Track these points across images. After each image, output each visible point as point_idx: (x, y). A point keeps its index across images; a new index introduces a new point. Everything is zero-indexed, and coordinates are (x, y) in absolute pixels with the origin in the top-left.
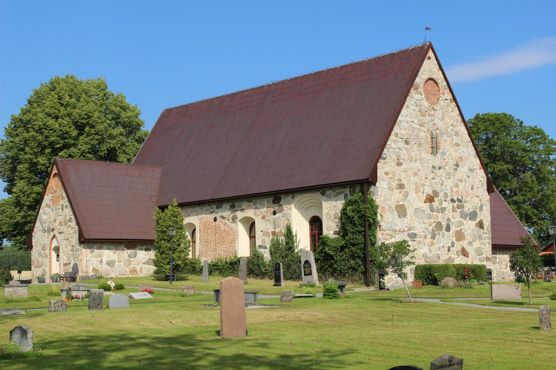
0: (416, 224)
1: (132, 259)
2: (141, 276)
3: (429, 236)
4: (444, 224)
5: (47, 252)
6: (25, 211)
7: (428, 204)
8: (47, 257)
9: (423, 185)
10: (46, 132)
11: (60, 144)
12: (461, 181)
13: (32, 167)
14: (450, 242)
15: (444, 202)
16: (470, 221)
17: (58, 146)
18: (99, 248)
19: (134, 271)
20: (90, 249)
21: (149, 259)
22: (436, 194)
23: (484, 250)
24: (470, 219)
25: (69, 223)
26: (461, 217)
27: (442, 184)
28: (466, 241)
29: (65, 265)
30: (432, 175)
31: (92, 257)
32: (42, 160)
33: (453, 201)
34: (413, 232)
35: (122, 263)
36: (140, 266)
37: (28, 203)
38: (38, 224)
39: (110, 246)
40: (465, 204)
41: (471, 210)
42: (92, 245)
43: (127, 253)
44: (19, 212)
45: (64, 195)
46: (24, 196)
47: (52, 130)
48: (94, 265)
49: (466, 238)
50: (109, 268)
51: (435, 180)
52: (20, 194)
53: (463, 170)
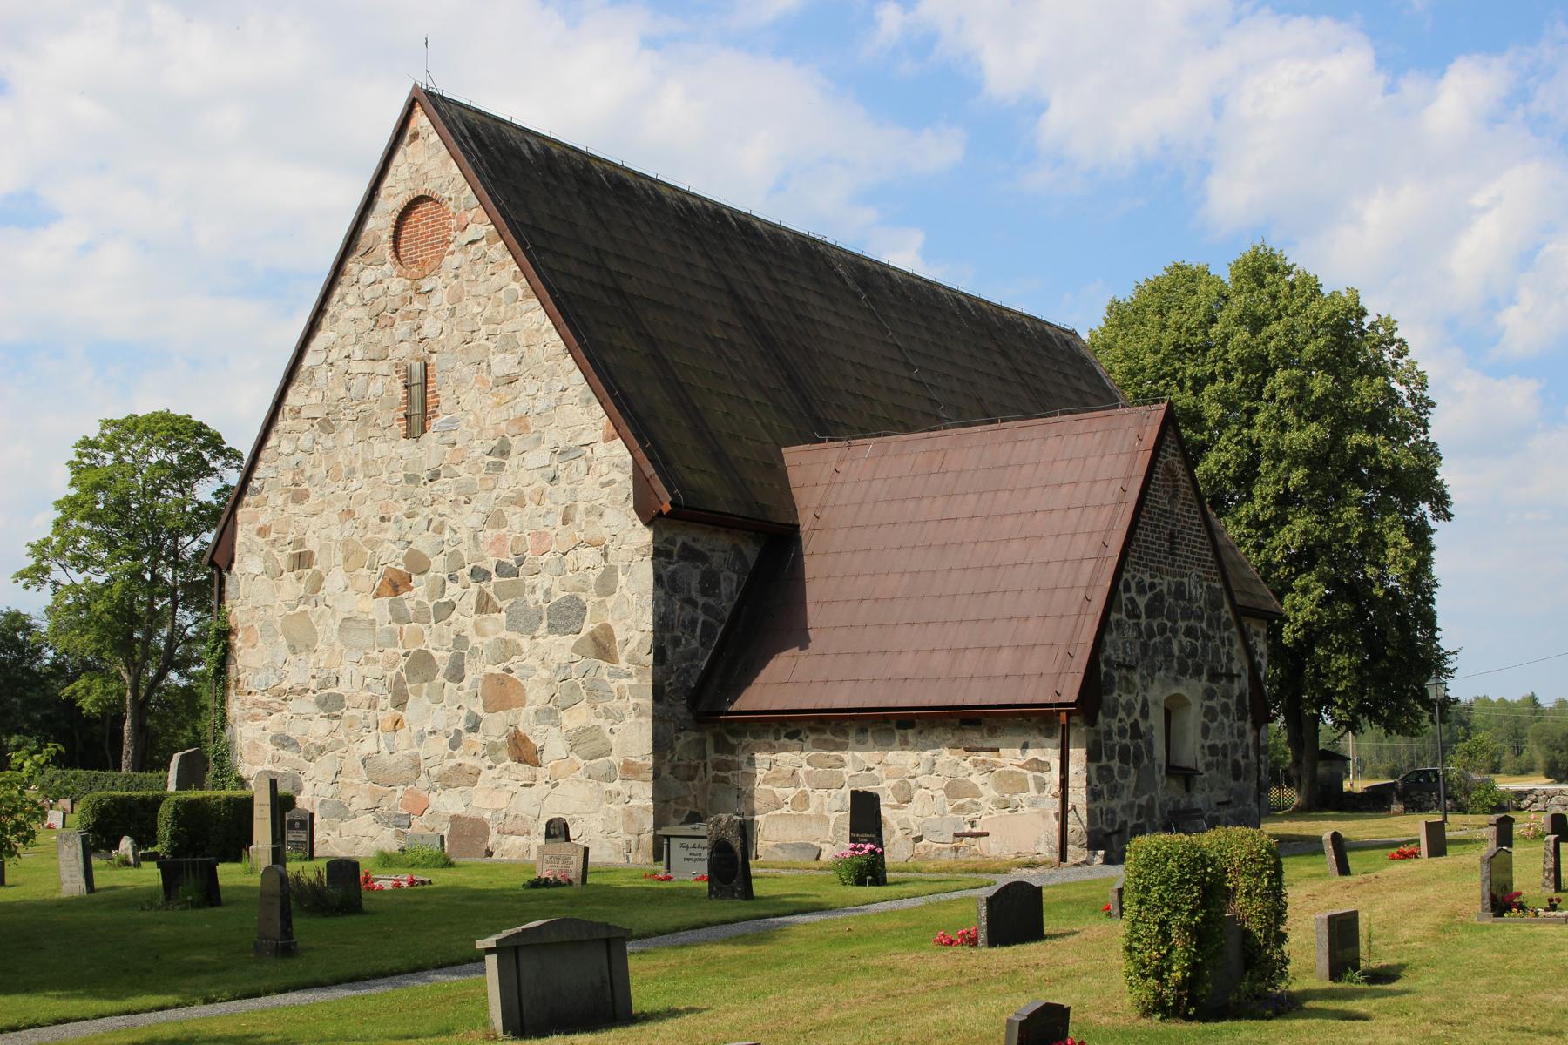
0: (346, 669)
3: (385, 702)
4: (442, 657)
7: (386, 600)
9: (373, 544)
12: (518, 501)
14: (463, 713)
15: (449, 584)
16: (551, 637)
22: (418, 563)
23: (613, 740)
24: (552, 628)
26: (511, 627)
27: (440, 530)
28: (529, 710)
30: (405, 505)
33: (479, 574)
34: (334, 690)
40: (528, 580)
41: (558, 595)
49: (531, 697)
51: (417, 519)
53: (529, 462)
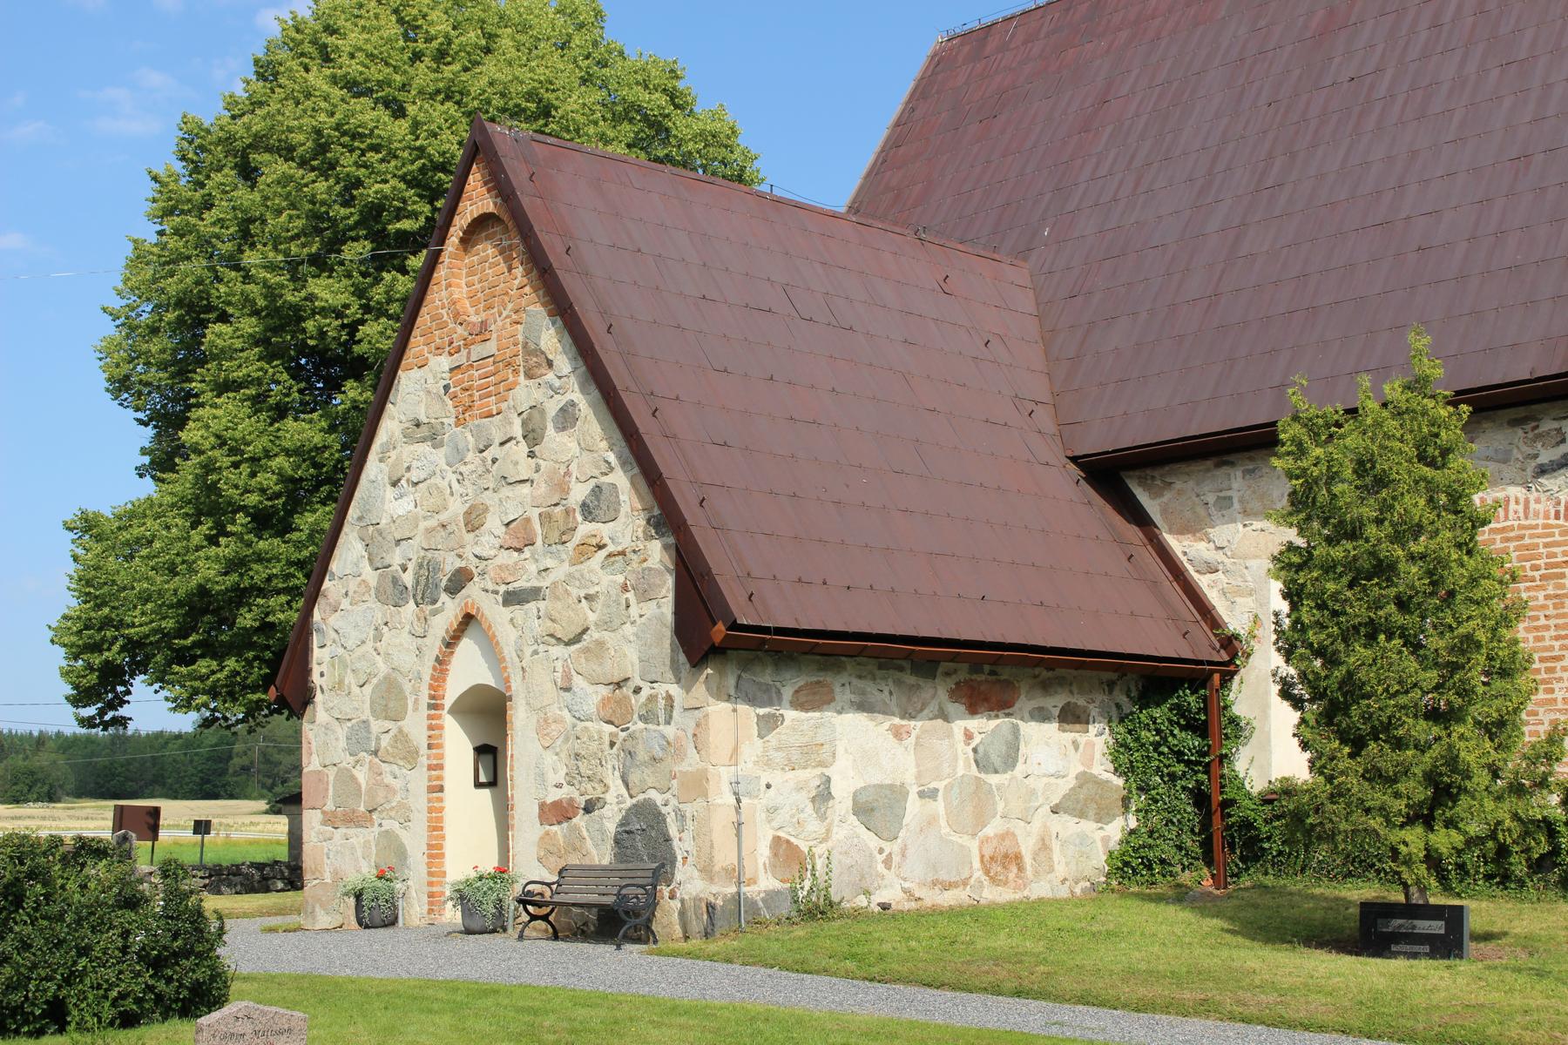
1: (993, 779)
2: (1040, 889)
5: (415, 725)
6: (239, 537)
8: (411, 756)
10: (347, 162)
11: (414, 215)
13: (276, 330)
17: (406, 225)
18: (810, 700)
19: (1004, 861)
20: (752, 701)
21: (1085, 779)
25: (585, 529)
29: (557, 813)
31: (768, 763)
32: (327, 290)
35: (939, 806)
36: (1036, 825)
37: (253, 499)
38: (349, 554)
39: (869, 687)
42: (766, 676)
43: (969, 736)
44: (213, 541)
45: (550, 338)
46: (236, 465)
47: (376, 148)
48: (780, 818)
50: (872, 841)
52: (217, 453)
